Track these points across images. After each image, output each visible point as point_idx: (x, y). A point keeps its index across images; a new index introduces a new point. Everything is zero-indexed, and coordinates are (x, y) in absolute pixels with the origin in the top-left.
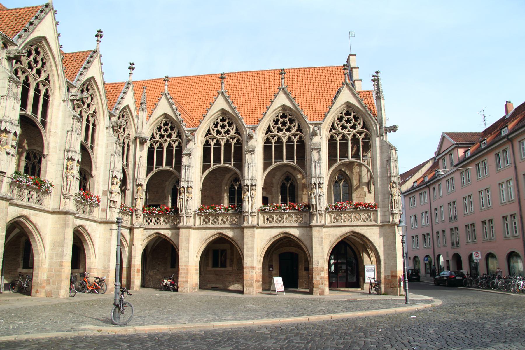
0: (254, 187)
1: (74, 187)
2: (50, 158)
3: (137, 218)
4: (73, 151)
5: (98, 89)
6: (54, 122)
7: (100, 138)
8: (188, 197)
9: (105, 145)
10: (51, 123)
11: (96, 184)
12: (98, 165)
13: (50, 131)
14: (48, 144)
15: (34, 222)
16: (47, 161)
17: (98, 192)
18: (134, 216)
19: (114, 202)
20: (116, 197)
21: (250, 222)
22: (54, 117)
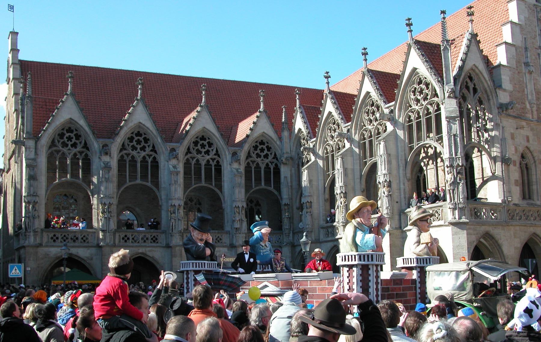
5: (214, 135)
6: (162, 180)
7: (225, 175)
8: (307, 213)
11: (226, 215)
12: (226, 198)
14: (161, 197)
15: (151, 256)
17: (228, 222)
22: (162, 176)
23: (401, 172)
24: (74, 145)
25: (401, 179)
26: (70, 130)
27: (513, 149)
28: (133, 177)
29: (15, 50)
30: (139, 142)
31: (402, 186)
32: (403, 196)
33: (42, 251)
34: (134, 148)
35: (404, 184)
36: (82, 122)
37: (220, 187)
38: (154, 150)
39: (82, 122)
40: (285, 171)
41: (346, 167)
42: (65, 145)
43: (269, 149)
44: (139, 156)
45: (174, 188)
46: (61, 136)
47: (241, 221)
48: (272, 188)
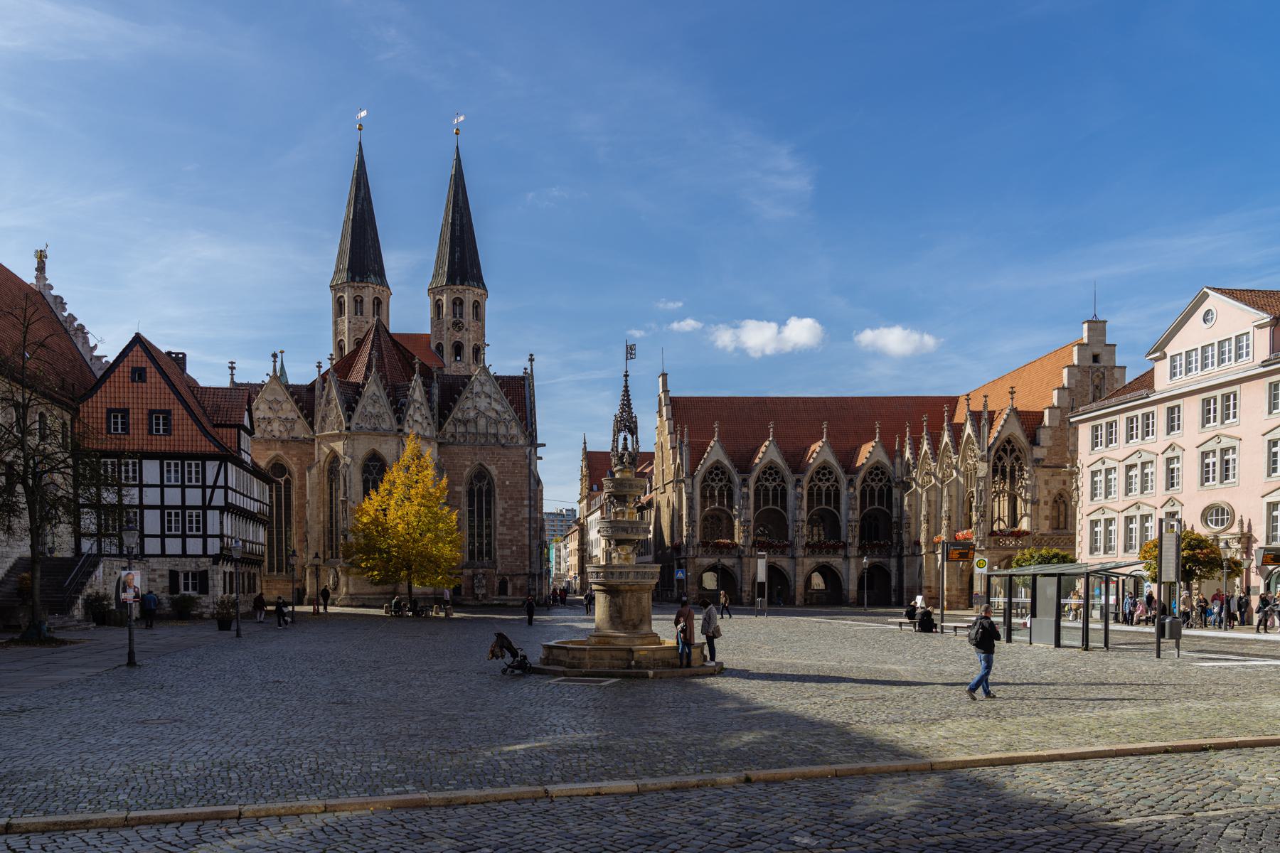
24: (721, 480)
26: (717, 468)
27: (1046, 492)
28: (766, 503)
29: (666, 391)
30: (771, 475)
33: (698, 561)
34: (767, 480)
36: (726, 462)
38: (783, 481)
39: (726, 462)
40: (896, 493)
42: (713, 480)
43: (883, 473)
44: (770, 485)
45: (799, 512)
46: (711, 473)
47: (854, 537)
48: (884, 508)
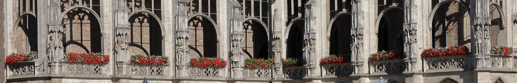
0: (360, 37)
1: (185, 59)
2: (166, 38)
3: (276, 71)
4: (180, 31)
6: (166, 9)
8: (311, 49)
9: (225, 11)
10: (163, 11)
13: (164, 17)
16: (164, 41)
17: (223, 55)
18: (274, 70)
19: (235, 62)
20: (236, 58)
21: (356, 72)
22: (165, 6)
23: (425, 21)
25: (425, 28)
31: (425, 34)
32: (425, 43)
35: (427, 33)
37: (214, 17)
41: (362, 10)
